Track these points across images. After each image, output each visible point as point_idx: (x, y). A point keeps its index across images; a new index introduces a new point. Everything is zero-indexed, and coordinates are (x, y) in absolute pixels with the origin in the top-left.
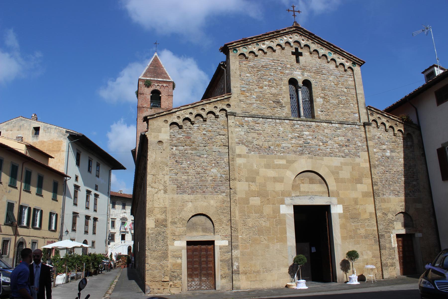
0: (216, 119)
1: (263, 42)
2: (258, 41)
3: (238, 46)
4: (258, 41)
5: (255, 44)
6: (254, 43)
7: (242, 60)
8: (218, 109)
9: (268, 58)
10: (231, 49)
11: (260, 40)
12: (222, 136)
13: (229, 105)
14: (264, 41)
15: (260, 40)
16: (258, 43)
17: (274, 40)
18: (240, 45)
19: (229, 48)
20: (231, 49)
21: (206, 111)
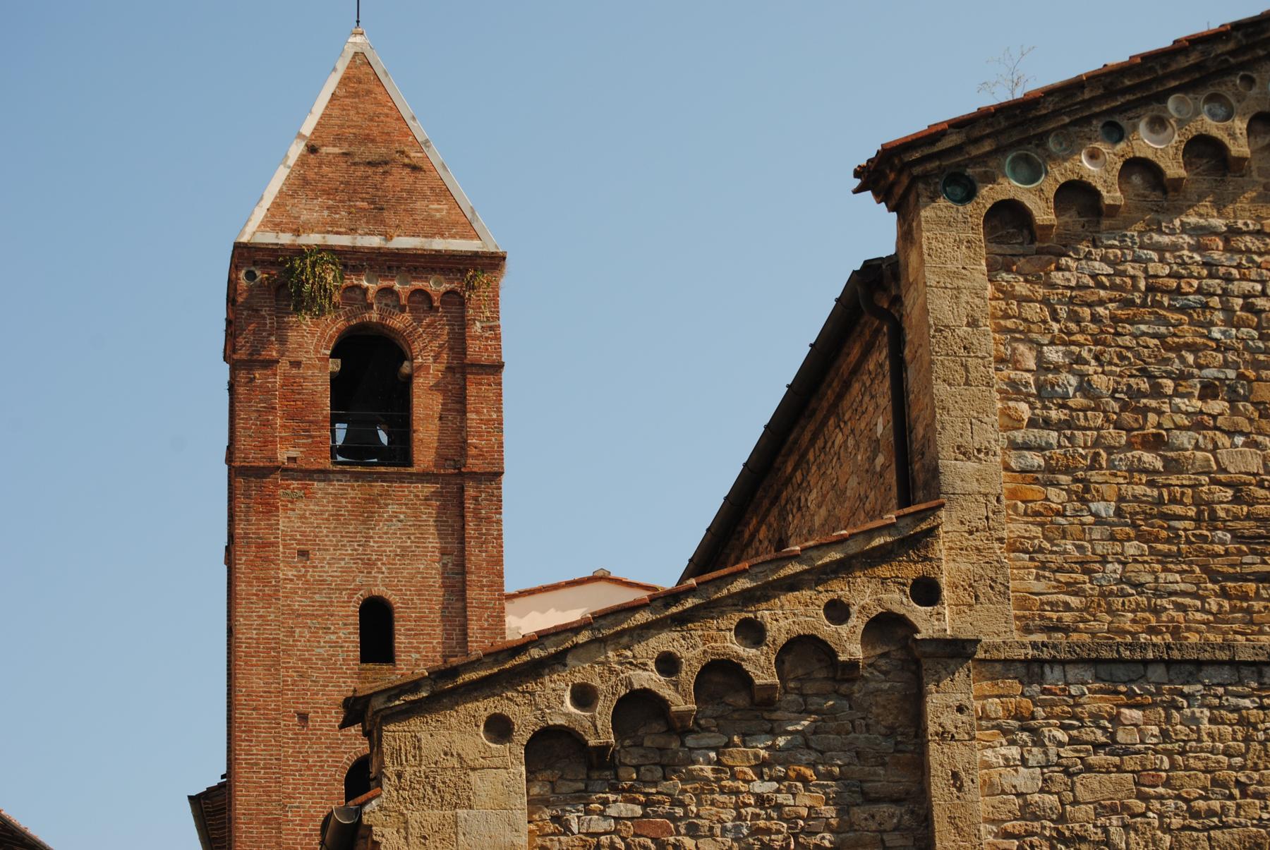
0: (844, 688)
1: (1154, 109)
2: (1120, 101)
3: (975, 151)
4: (1120, 101)
5: (1097, 124)
6: (1087, 120)
7: (1006, 249)
8: (853, 620)
9: (1193, 220)
10: (925, 177)
11: (1130, 97)
12: (885, 809)
13: (927, 592)
14: (1162, 98)
15: (1130, 97)
16: (1117, 119)
17: (1231, 86)
18: (987, 147)
19: (917, 170)
20: (925, 177)
21: (769, 639)
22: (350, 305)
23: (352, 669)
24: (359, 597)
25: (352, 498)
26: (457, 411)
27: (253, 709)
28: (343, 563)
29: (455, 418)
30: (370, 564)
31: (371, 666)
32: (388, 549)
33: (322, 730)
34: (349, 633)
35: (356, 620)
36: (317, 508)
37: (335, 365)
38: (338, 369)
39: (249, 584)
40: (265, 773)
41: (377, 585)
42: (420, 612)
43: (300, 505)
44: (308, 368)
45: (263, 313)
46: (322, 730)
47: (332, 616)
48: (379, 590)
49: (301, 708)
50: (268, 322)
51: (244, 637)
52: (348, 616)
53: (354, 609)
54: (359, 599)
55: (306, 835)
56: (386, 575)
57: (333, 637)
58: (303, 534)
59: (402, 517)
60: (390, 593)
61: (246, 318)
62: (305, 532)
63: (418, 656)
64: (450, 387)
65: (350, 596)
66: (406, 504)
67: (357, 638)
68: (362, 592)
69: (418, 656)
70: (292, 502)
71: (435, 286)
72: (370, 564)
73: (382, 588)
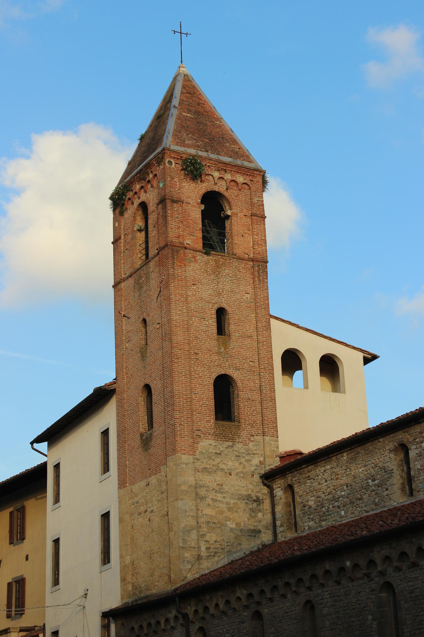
22: (208, 182)
23: (214, 337)
24: (216, 307)
28: (209, 291)
32: (226, 288)
33: (204, 362)
34: (213, 322)
36: (199, 267)
37: (203, 207)
39: (175, 295)
40: (185, 378)
41: (222, 303)
42: (239, 316)
43: (192, 264)
45: (176, 180)
46: (204, 362)
47: (206, 313)
50: (178, 184)
51: (174, 318)
52: (212, 314)
53: (214, 312)
54: (216, 307)
55: (200, 406)
56: (226, 299)
60: (227, 307)
61: (169, 181)
62: (195, 276)
64: (246, 224)
66: (232, 270)
68: (217, 305)
69: (238, 335)
70: (189, 263)
71: (240, 179)
72: (219, 294)
73: (224, 304)
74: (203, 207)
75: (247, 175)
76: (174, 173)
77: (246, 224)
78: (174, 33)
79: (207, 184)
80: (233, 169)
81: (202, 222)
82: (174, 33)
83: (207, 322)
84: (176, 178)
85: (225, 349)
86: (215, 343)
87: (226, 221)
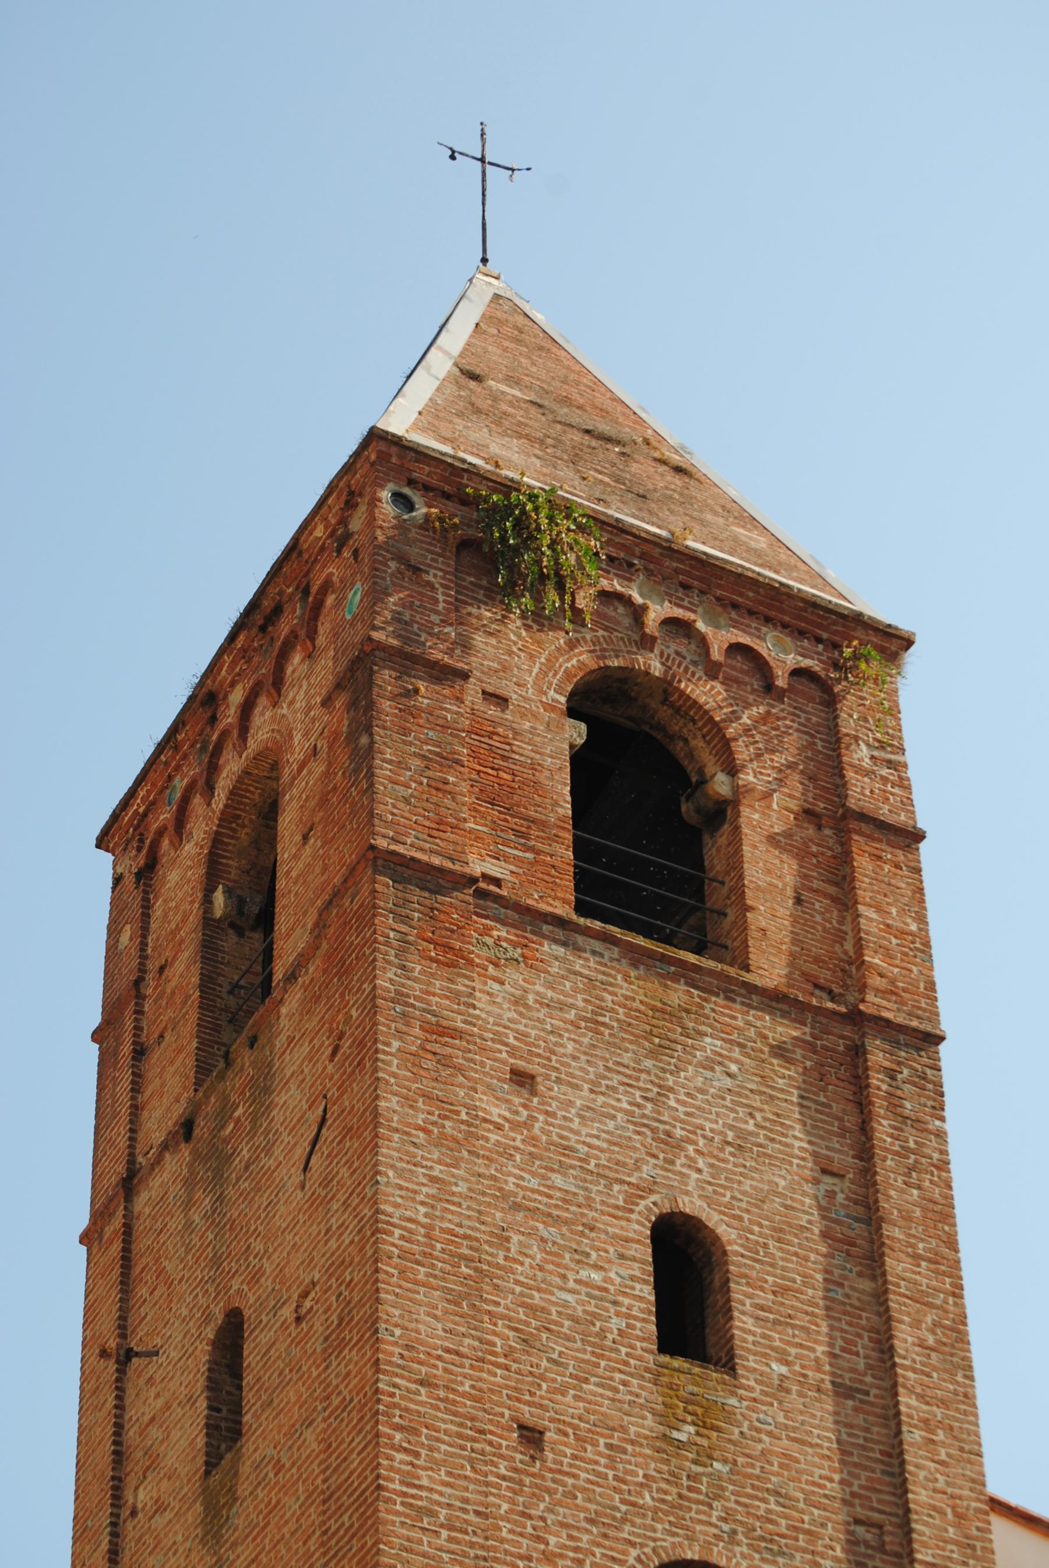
22: (606, 629)
23: (640, 1359)
25: (626, 998)
26: (834, 899)
27: (421, 1383)
28: (611, 1125)
29: (828, 911)
30: (670, 1143)
31: (678, 1362)
32: (708, 1125)
33: (575, 1476)
34: (632, 1278)
35: (645, 1252)
38: (580, 741)
39: (408, 1101)
40: (450, 1540)
41: (687, 1193)
42: (783, 1278)
44: (523, 716)
46: (575, 1476)
47: (592, 1229)
48: (691, 1204)
49: (528, 1414)
50: (441, 598)
51: (398, 1213)
52: (627, 1240)
53: (640, 1229)
54: (649, 1210)
56: (706, 1176)
57: (596, 1276)
58: (521, 1036)
59: (734, 1068)
60: (716, 1217)
61: (392, 575)
62: (527, 1035)
63: (784, 1370)
64: (814, 849)
65: (631, 1200)
67: (648, 1292)
68: (654, 1198)
73: (699, 1203)
74: (577, 732)
75: (819, 640)
76: (422, 549)
77: (814, 849)
78: (453, 157)
79: (601, 633)
80: (741, 595)
81: (572, 792)
82: (453, 157)
83: (596, 1276)
84: (432, 571)
85: (703, 1425)
86: (645, 1391)
87: (707, 839)
